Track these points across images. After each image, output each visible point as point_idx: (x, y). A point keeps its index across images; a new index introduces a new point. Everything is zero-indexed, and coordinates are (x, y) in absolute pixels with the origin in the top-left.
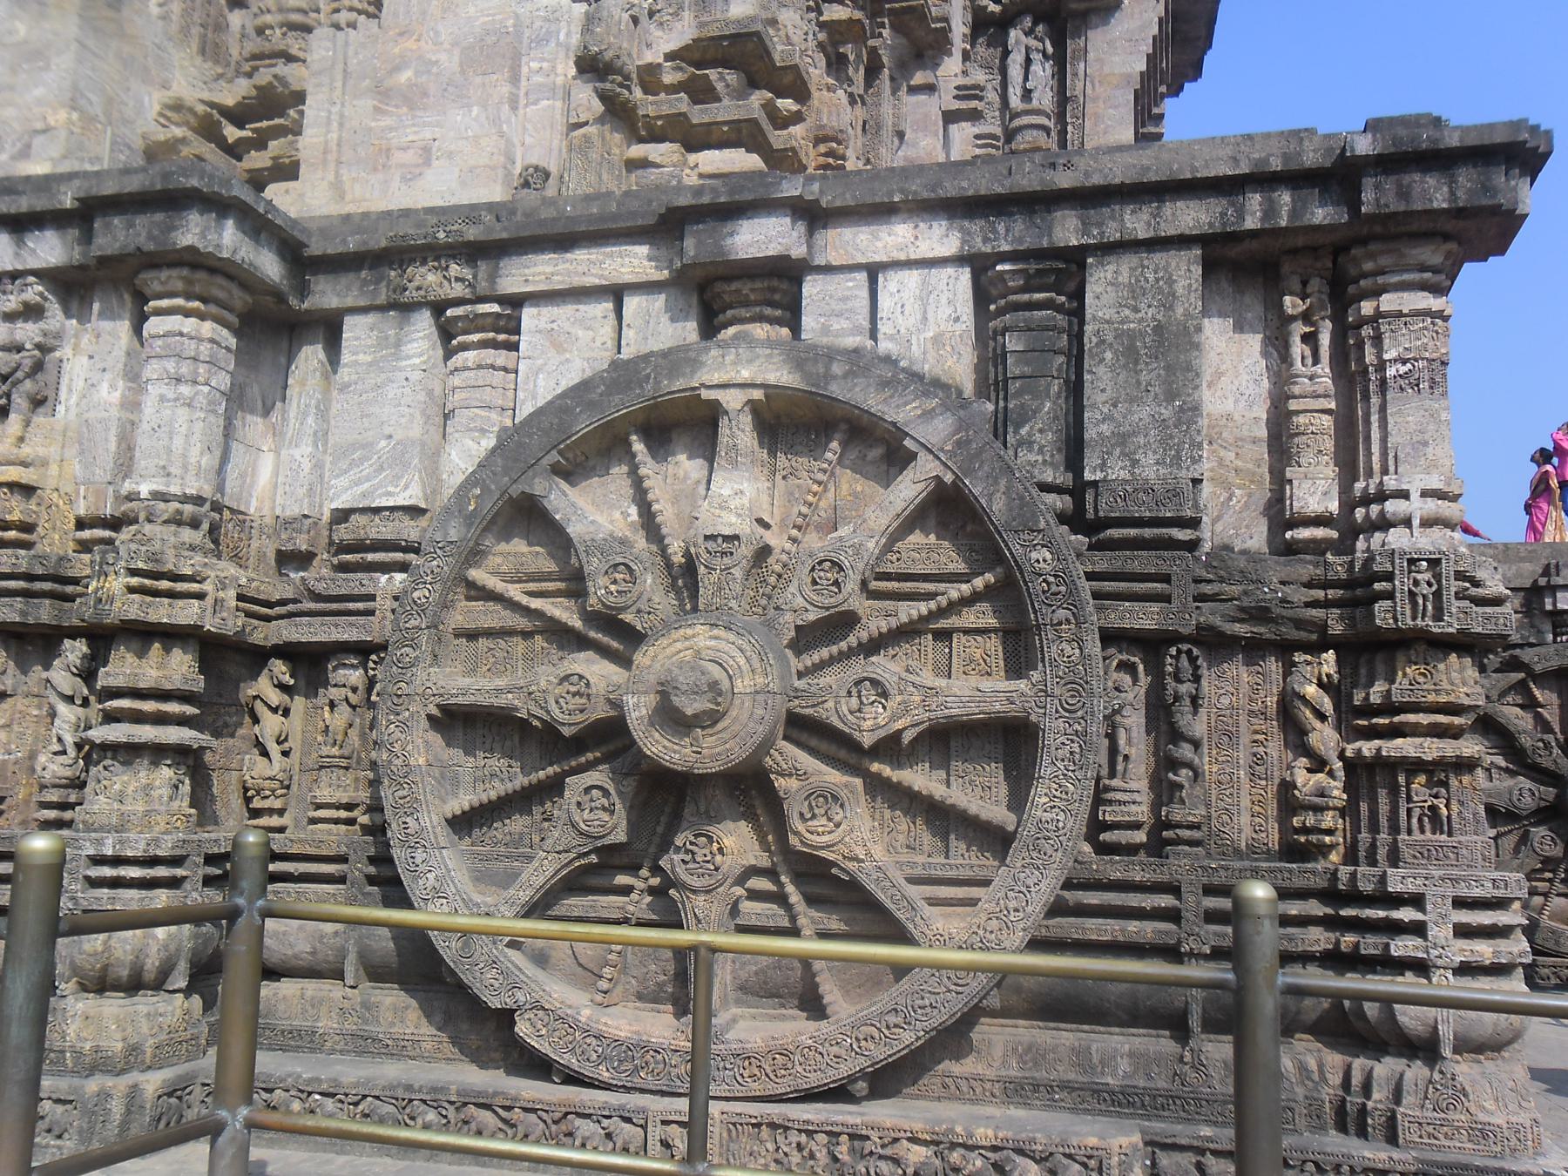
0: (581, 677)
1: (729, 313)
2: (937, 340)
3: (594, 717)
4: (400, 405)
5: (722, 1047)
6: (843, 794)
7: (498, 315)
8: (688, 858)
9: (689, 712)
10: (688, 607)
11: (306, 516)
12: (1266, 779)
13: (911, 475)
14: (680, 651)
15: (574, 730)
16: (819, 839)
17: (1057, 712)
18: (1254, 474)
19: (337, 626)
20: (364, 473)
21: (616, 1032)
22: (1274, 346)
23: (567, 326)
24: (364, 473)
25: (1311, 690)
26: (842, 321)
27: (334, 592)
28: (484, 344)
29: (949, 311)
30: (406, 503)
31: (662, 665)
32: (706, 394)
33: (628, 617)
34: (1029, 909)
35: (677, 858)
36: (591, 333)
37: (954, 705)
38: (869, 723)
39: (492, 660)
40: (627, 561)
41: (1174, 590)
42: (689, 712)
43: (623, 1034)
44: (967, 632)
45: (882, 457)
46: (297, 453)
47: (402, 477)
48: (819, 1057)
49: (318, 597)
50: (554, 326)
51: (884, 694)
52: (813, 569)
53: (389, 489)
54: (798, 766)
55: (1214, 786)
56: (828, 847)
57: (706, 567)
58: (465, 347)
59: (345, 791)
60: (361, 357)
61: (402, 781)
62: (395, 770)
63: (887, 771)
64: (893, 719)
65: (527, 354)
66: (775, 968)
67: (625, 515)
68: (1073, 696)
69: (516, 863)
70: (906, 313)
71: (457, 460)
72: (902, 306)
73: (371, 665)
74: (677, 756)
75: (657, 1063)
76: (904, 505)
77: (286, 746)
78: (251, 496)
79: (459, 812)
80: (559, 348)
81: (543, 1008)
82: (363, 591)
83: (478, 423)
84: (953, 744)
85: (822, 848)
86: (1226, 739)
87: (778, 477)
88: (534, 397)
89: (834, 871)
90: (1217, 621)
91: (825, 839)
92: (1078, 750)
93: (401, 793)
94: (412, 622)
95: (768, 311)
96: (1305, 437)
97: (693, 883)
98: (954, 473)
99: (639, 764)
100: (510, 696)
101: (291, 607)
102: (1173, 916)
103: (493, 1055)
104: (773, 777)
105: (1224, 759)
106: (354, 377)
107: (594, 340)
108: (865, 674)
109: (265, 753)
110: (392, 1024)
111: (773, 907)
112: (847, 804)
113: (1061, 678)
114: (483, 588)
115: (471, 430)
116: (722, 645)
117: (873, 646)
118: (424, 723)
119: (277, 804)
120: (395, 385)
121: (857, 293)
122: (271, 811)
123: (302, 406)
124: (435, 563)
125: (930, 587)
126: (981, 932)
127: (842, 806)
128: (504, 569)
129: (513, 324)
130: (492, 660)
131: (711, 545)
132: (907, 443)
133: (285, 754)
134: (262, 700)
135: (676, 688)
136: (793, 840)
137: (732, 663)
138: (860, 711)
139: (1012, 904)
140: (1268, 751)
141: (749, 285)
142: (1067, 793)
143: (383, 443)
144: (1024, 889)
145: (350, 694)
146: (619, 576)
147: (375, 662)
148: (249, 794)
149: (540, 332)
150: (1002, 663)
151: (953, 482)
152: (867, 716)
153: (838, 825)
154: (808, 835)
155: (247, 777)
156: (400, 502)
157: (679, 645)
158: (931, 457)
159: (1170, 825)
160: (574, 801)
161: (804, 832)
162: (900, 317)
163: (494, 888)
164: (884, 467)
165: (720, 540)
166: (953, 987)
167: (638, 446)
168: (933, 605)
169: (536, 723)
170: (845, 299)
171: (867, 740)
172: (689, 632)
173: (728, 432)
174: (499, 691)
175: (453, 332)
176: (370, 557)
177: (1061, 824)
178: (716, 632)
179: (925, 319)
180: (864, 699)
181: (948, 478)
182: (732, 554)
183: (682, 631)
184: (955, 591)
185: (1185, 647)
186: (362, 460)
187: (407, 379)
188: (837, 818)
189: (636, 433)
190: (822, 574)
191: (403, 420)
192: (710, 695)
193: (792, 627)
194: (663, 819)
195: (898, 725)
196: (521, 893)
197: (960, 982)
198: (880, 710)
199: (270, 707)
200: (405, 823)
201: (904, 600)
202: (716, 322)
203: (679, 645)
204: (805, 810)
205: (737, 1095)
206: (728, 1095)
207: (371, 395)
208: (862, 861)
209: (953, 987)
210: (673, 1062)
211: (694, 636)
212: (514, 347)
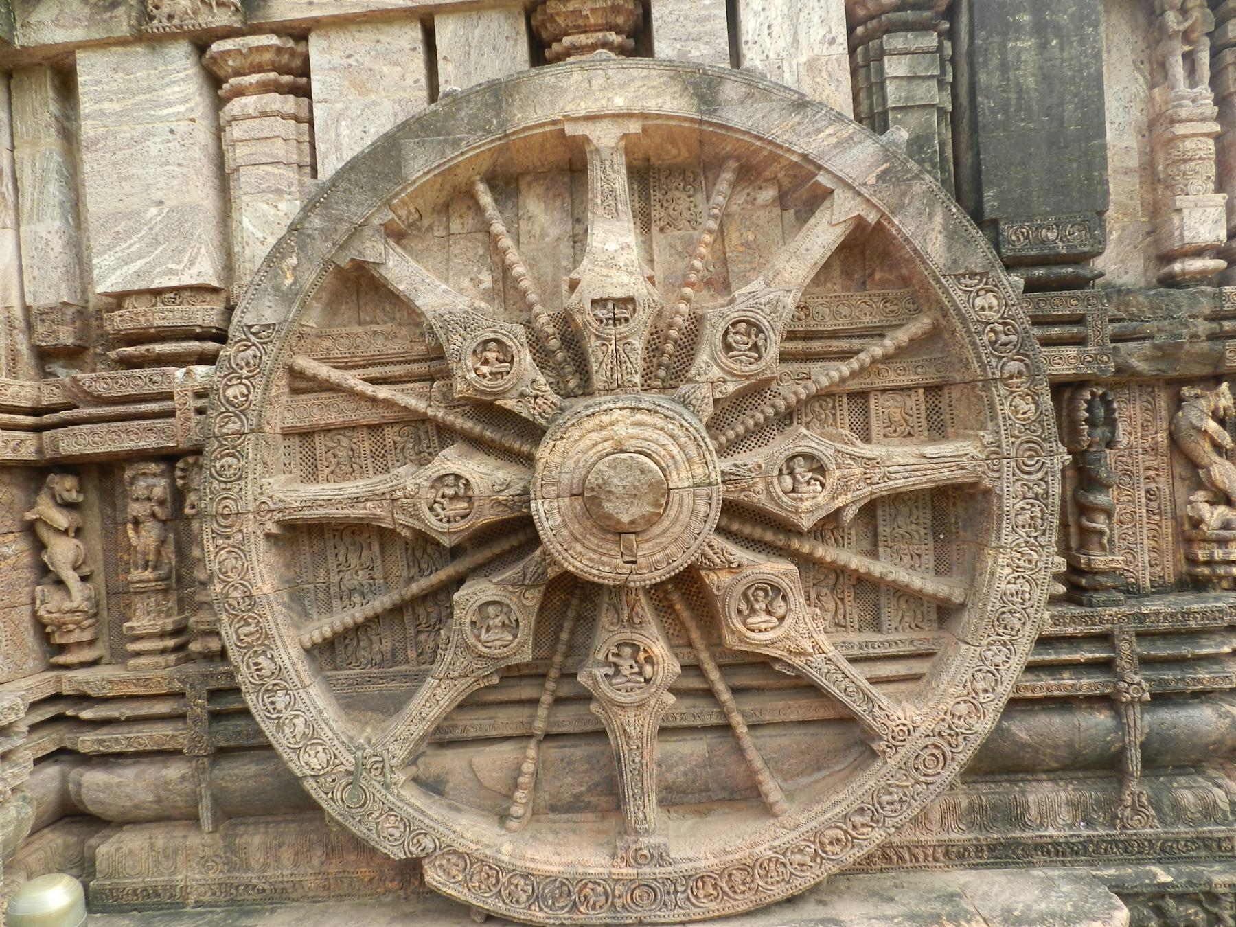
0: (458, 477)
1: (567, 41)
2: (811, 65)
3: (480, 522)
4: (167, 164)
5: (670, 869)
6: (785, 584)
7: (279, 50)
8: (611, 671)
9: (625, 519)
10: (572, 383)
11: (65, 304)
12: (1160, 514)
13: (828, 216)
14: (597, 444)
15: (455, 540)
16: (762, 636)
18: (1127, 205)
19: (128, 432)
20: (134, 248)
21: (548, 868)
22: (1139, 69)
23: (367, 62)
24: (134, 248)
25: (1212, 426)
26: (702, 46)
27: (119, 392)
28: (265, 88)
29: (822, 31)
30: (194, 282)
31: (577, 463)
32: (570, 130)
33: (509, 403)
34: (1000, 689)
35: (599, 672)
36: (399, 69)
37: (898, 476)
39: (334, 461)
40: (499, 336)
42: (625, 519)
43: (554, 869)
45: (774, 201)
46: (41, 229)
47: (184, 250)
48: (781, 869)
49: (100, 401)
50: (352, 61)
51: (822, 470)
52: (726, 333)
53: (170, 266)
54: (731, 558)
56: (773, 643)
57: (598, 337)
58: (240, 92)
59: (169, 616)
60: (107, 106)
61: (246, 615)
62: (235, 603)
63: (820, 551)
65: (321, 97)
66: (705, 765)
67: (476, 282)
68: (1030, 457)
69: (393, 684)
70: (774, 34)
71: (252, 229)
72: (769, 27)
73: (178, 473)
74: (607, 569)
75: (597, 895)
76: (822, 250)
77: (86, 570)
79: (320, 640)
80: (362, 89)
81: (455, 852)
82: (156, 389)
83: (271, 183)
84: (880, 513)
85: (766, 646)
86: (1126, 479)
87: (655, 229)
88: (338, 149)
89: (778, 667)
91: (770, 635)
92: (1039, 515)
93: (246, 630)
94: (231, 426)
95: (613, 37)
96: (1193, 164)
97: (623, 700)
98: (879, 210)
99: (544, 573)
100: (369, 504)
101: (64, 414)
102: (1106, 666)
103: (389, 885)
104: (703, 573)
106: (101, 130)
107: (403, 78)
108: (799, 449)
109: (60, 583)
110: (266, 865)
111: (702, 705)
112: (790, 595)
113: (1017, 437)
114: (314, 378)
115: (264, 191)
116: (648, 433)
117: (787, 418)
118: (263, 545)
119: (87, 636)
120: (157, 139)
121: (716, 12)
122: (80, 645)
123: (39, 172)
124: (250, 352)
125: (844, 344)
126: (949, 718)
127: (784, 598)
128: (335, 353)
129: (297, 62)
130: (334, 461)
131: (601, 313)
132: (822, 178)
133: (84, 579)
134: (45, 523)
135: (610, 492)
136: (731, 641)
137: (663, 453)
138: (793, 491)
139: (980, 686)
140: (1160, 486)
142: (1030, 562)
143: (153, 211)
144: (992, 669)
145: (157, 509)
146: (491, 355)
147: (183, 470)
148: (48, 630)
149: (335, 69)
150: (924, 422)
151: (878, 223)
152: (805, 496)
153: (781, 619)
154: (749, 634)
155: (42, 612)
156: (186, 280)
157: (595, 436)
158: (850, 194)
159: (1082, 573)
160: (468, 621)
161: (744, 630)
162: (768, 41)
163: (370, 714)
164: (777, 211)
165: (610, 306)
166: (923, 779)
167: (486, 199)
168: (855, 364)
169: (405, 533)
170: (702, 20)
171: (806, 523)
172: (605, 419)
173: (601, 174)
174: (354, 501)
175: (222, 74)
176: (158, 348)
177: (1027, 596)
178: (639, 417)
179: (796, 41)
180: (798, 476)
181: (872, 218)
182: (627, 320)
183: (596, 420)
184: (877, 349)
186: (129, 233)
187: (172, 131)
188: (781, 612)
189: (482, 180)
190: (738, 337)
191: (175, 182)
192: (651, 497)
193: (711, 402)
194: (567, 625)
195: (839, 503)
196: (413, 728)
197: (930, 772)
198: (819, 488)
199: (57, 531)
200: (256, 664)
201: (818, 360)
202: (547, 53)
203: (595, 436)
204: (744, 606)
205: (694, 918)
206: (683, 919)
207: (127, 152)
208: (810, 655)
209: (923, 779)
210: (617, 893)
211: (612, 424)
212: (304, 92)
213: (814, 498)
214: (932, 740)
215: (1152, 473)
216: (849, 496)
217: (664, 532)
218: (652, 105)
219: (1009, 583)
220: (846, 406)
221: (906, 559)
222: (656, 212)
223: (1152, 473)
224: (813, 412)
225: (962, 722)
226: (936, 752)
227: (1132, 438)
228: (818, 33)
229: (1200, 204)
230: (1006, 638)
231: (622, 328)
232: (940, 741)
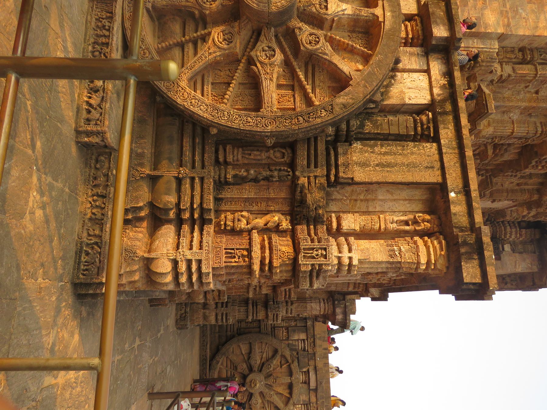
18: (355, 206)
34: (192, 107)
38: (259, 54)
44: (294, 96)
64: (261, 63)
68: (270, 123)
72: (414, 81)
84: (253, 90)
91: (216, 39)
95: (410, 36)
104: (238, 21)
108: (277, 52)
112: (229, 46)
138: (263, 51)
139: (193, 101)
141: (420, 29)
144: (199, 105)
151: (350, 85)
153: (221, 43)
165: (326, 5)
168: (303, 79)
171: (253, 54)
177: (223, 118)
179: (410, 88)
195: (259, 65)
204: (227, 32)
213: (261, 56)
214: (176, 85)
216: (261, 68)
218: (387, 23)
219: (228, 113)
220: (289, 83)
221: (236, 99)
222: (354, 35)
224: (288, 73)
226: (172, 86)
228: (413, 95)
229: (356, 221)
230: (209, 110)
231: (318, 6)
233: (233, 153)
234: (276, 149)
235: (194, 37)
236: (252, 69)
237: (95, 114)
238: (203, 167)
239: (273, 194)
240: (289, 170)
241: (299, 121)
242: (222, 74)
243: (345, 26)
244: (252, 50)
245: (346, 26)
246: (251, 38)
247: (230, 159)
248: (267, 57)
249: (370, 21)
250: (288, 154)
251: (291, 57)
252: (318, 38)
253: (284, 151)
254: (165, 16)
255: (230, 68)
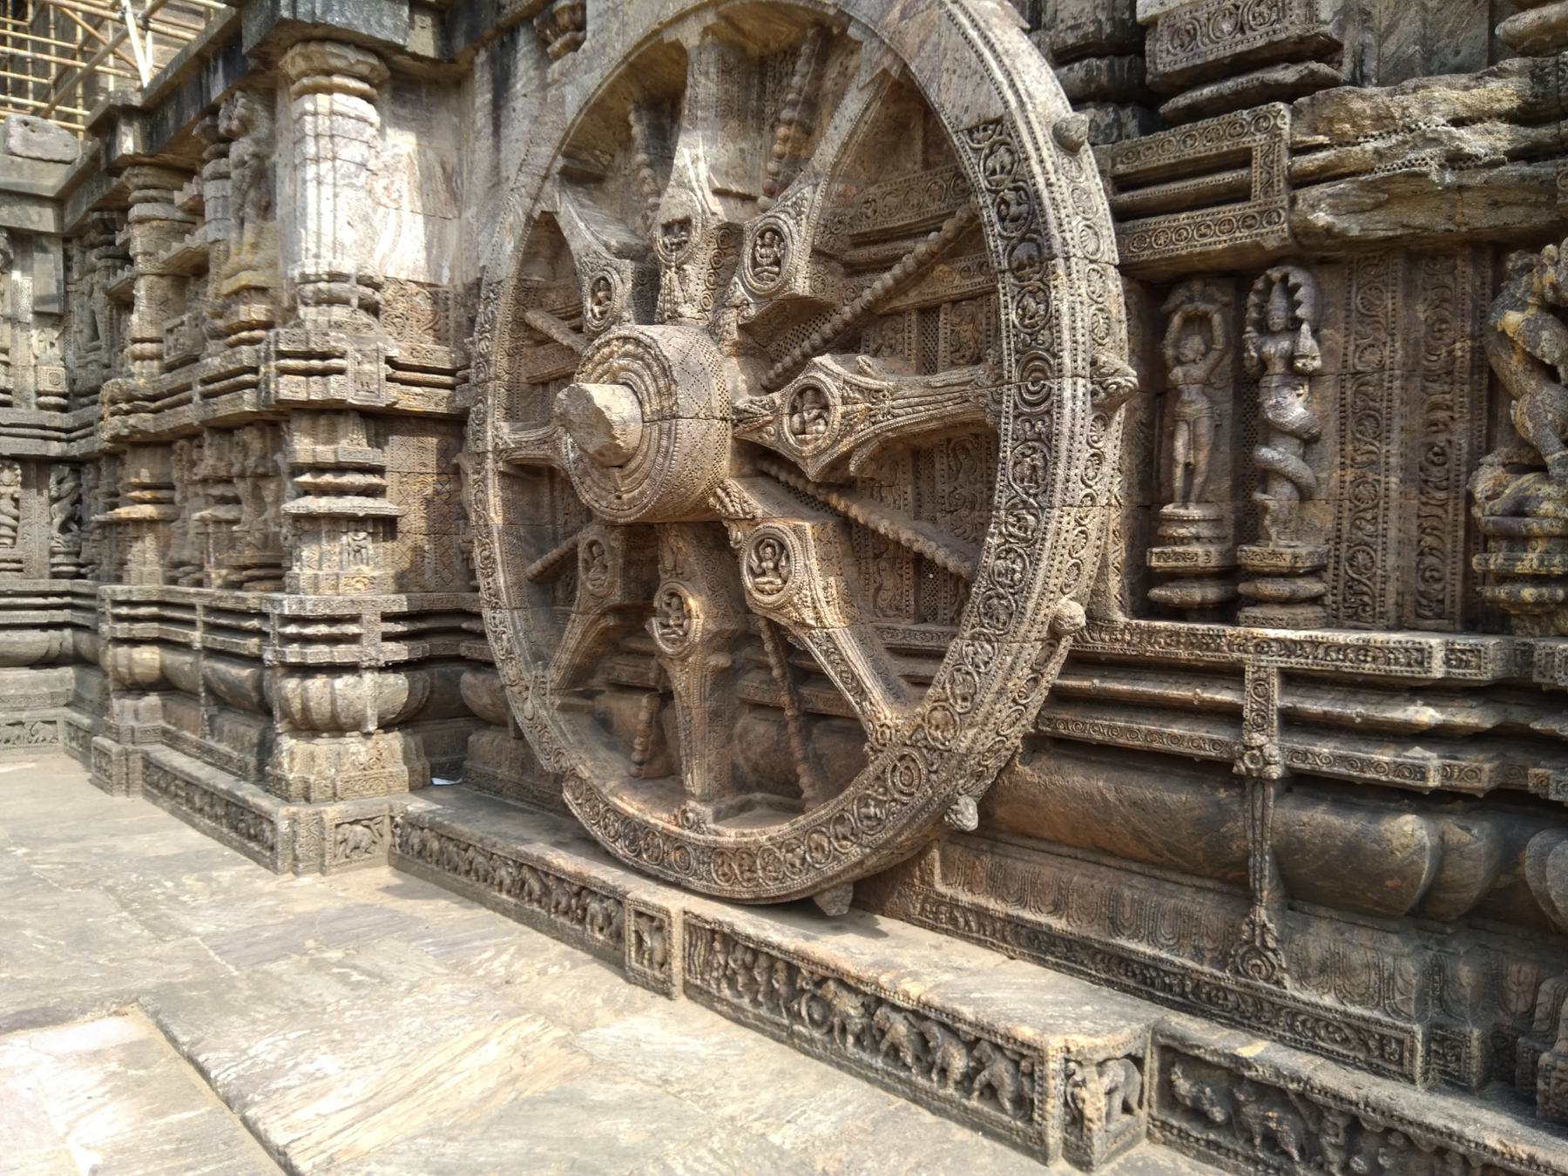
17: (1016, 407)
37: (901, 412)
38: (811, 447)
41: (1256, 174)
55: (1347, 504)
78: (441, 267)
90: (1322, 218)
104: (725, 524)
105: (1364, 458)
127: (788, 558)
138: (804, 432)
140: (1454, 438)
171: (812, 470)
177: (1017, 576)
185: (1275, 274)
189: (637, 109)
195: (843, 447)
208: (811, 627)
215: (1441, 415)
217: (638, 467)
219: (999, 558)
220: (914, 326)
223: (1441, 415)
225: (938, 734)
226: (912, 765)
227: (1387, 352)
232: (915, 754)
233: (1182, 541)
234: (1170, 352)
235: (783, 675)
236: (861, 468)
237: (1001, 1070)
238: (1232, 674)
239: (1387, 352)
240: (1259, 285)
241: (1030, 258)
242: (888, 583)
243: (742, 150)
244: (801, 474)
245: (744, 145)
246: (777, 479)
247: (1204, 555)
248: (819, 416)
249: (722, 58)
250: (1191, 300)
251: (827, 329)
252: (762, 236)
253: (1177, 320)
254: (734, 766)
255: (870, 554)
